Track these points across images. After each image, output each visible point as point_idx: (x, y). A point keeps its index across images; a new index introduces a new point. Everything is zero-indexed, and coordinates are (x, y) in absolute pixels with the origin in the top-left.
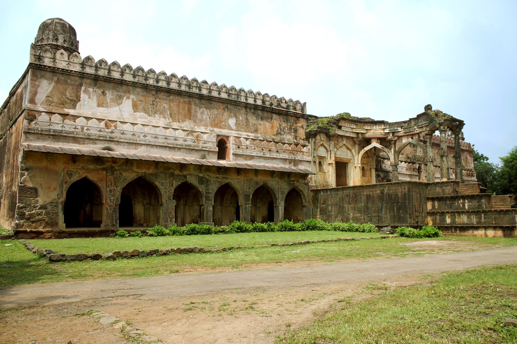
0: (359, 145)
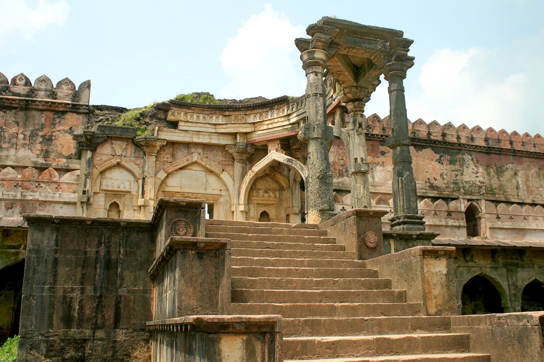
0: (241, 161)
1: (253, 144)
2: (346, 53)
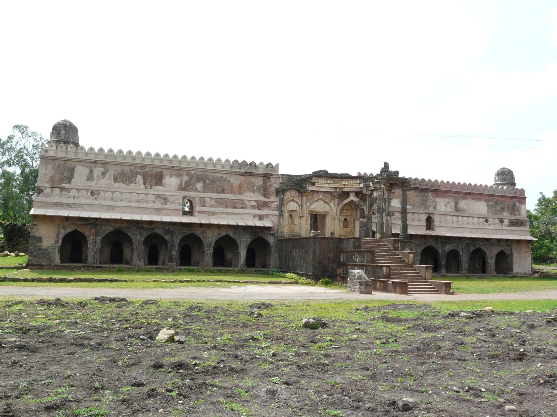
0: (339, 198)
1: (343, 192)
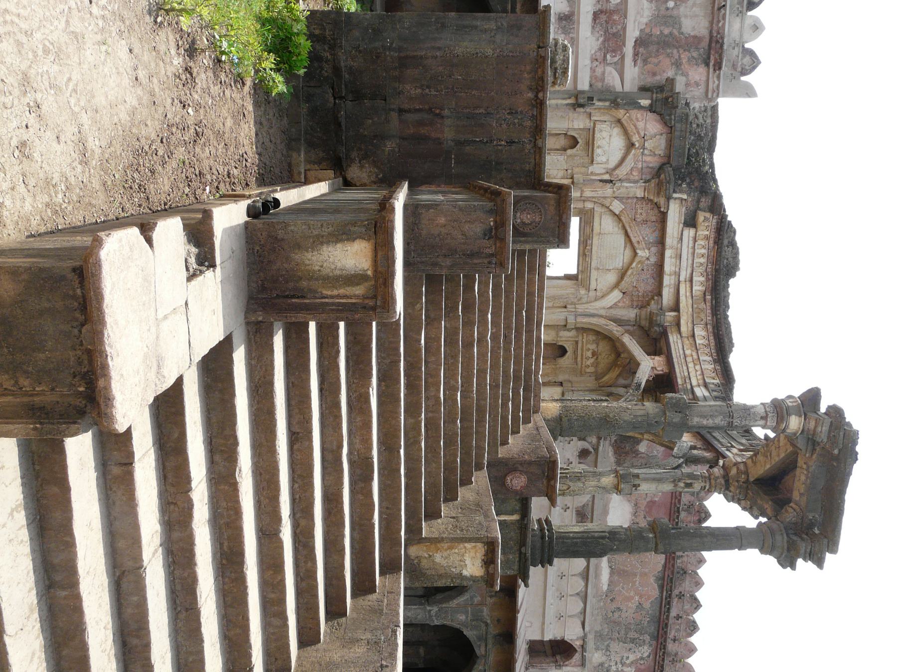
1: (664, 334)
2: (799, 465)
